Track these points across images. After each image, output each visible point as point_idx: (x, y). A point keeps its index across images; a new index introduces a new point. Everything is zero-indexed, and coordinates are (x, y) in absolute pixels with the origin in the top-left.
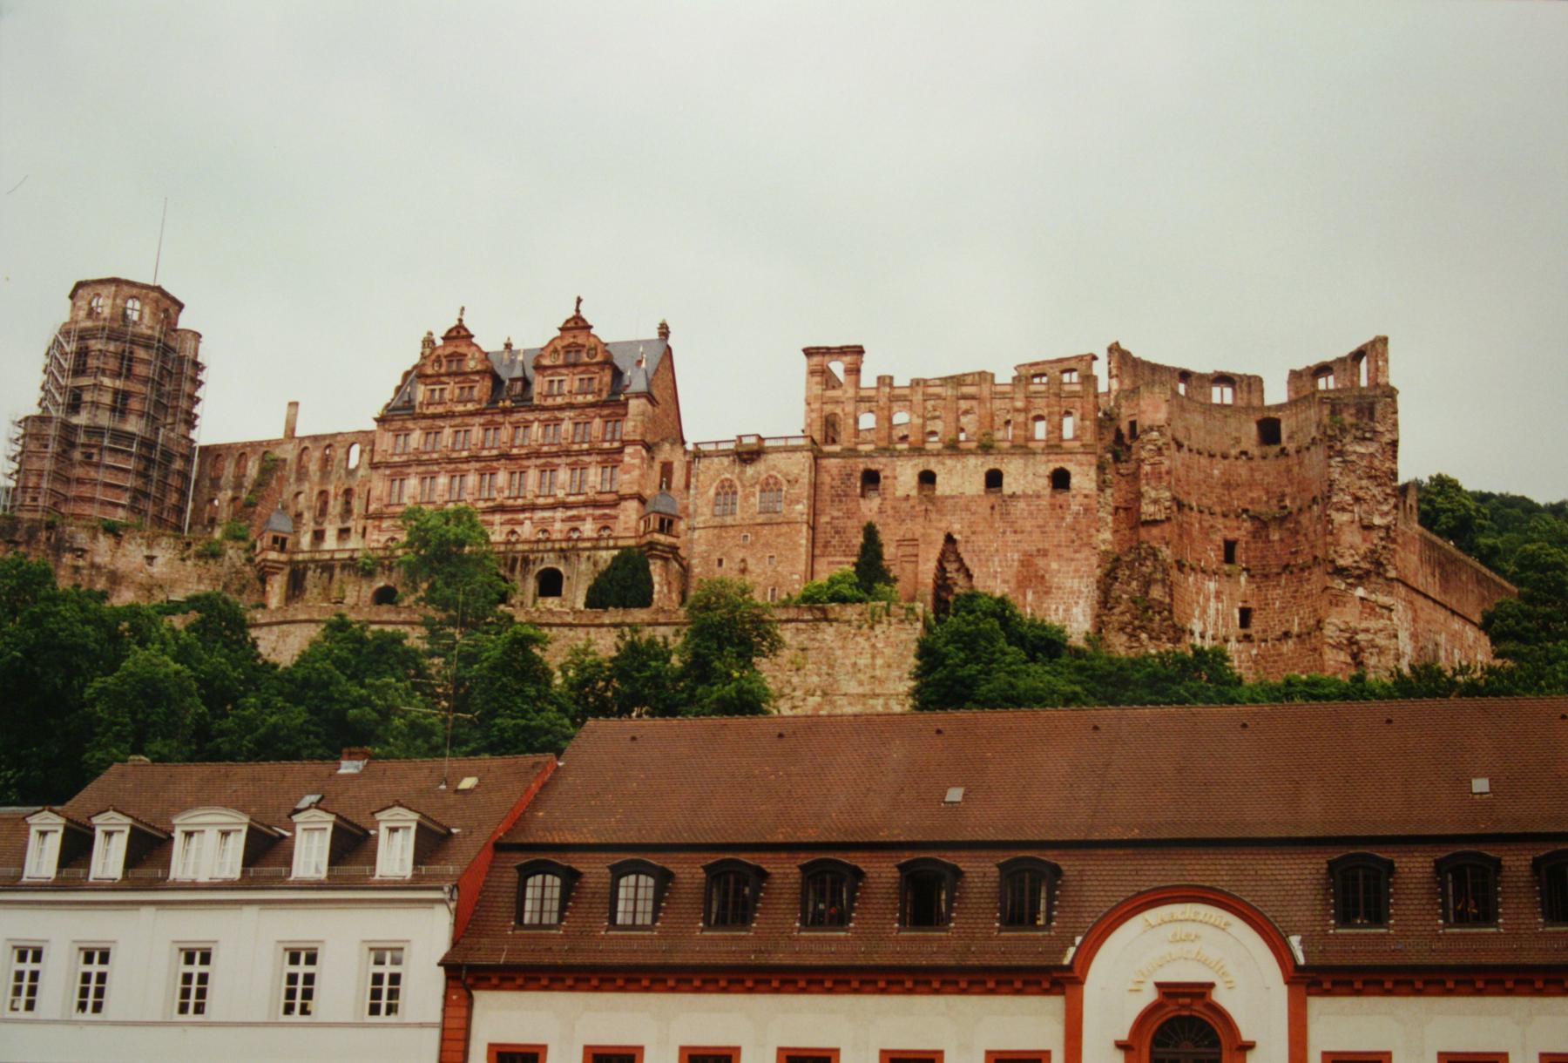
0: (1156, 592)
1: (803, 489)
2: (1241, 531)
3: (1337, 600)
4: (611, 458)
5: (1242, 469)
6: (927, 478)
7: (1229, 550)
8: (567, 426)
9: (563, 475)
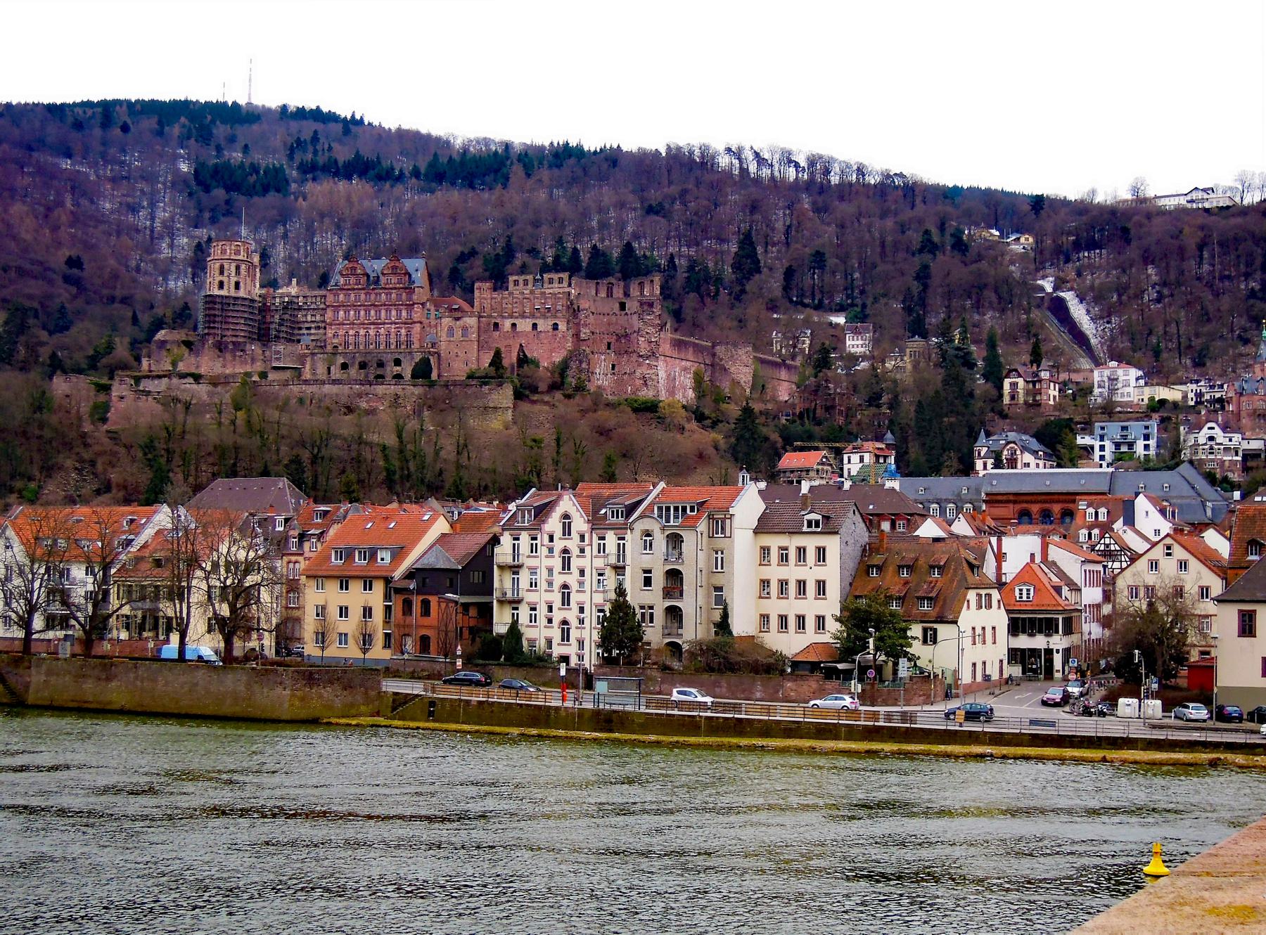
0: (584, 365)
1: (475, 329)
2: (613, 341)
3: (640, 365)
4: (410, 307)
5: (614, 318)
6: (514, 325)
7: (609, 344)
8: (394, 296)
9: (394, 313)
